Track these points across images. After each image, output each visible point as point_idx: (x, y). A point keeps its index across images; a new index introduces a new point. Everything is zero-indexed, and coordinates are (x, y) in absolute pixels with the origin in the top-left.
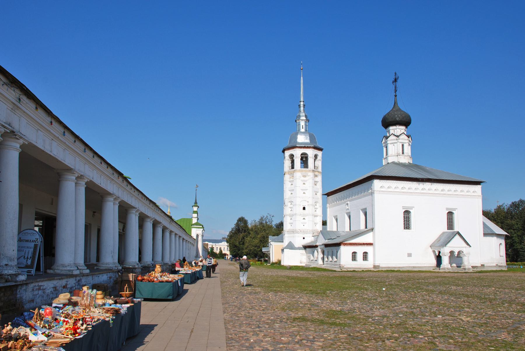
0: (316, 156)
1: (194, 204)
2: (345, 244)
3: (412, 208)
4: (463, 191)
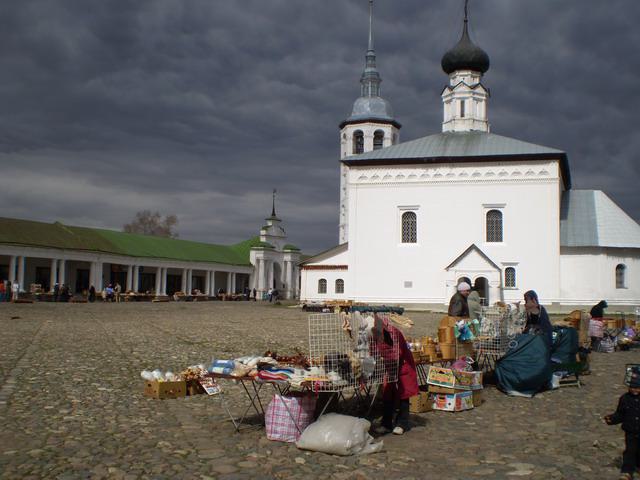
0: (379, 136)
1: (270, 216)
2: (308, 268)
3: (417, 207)
4: (519, 173)
